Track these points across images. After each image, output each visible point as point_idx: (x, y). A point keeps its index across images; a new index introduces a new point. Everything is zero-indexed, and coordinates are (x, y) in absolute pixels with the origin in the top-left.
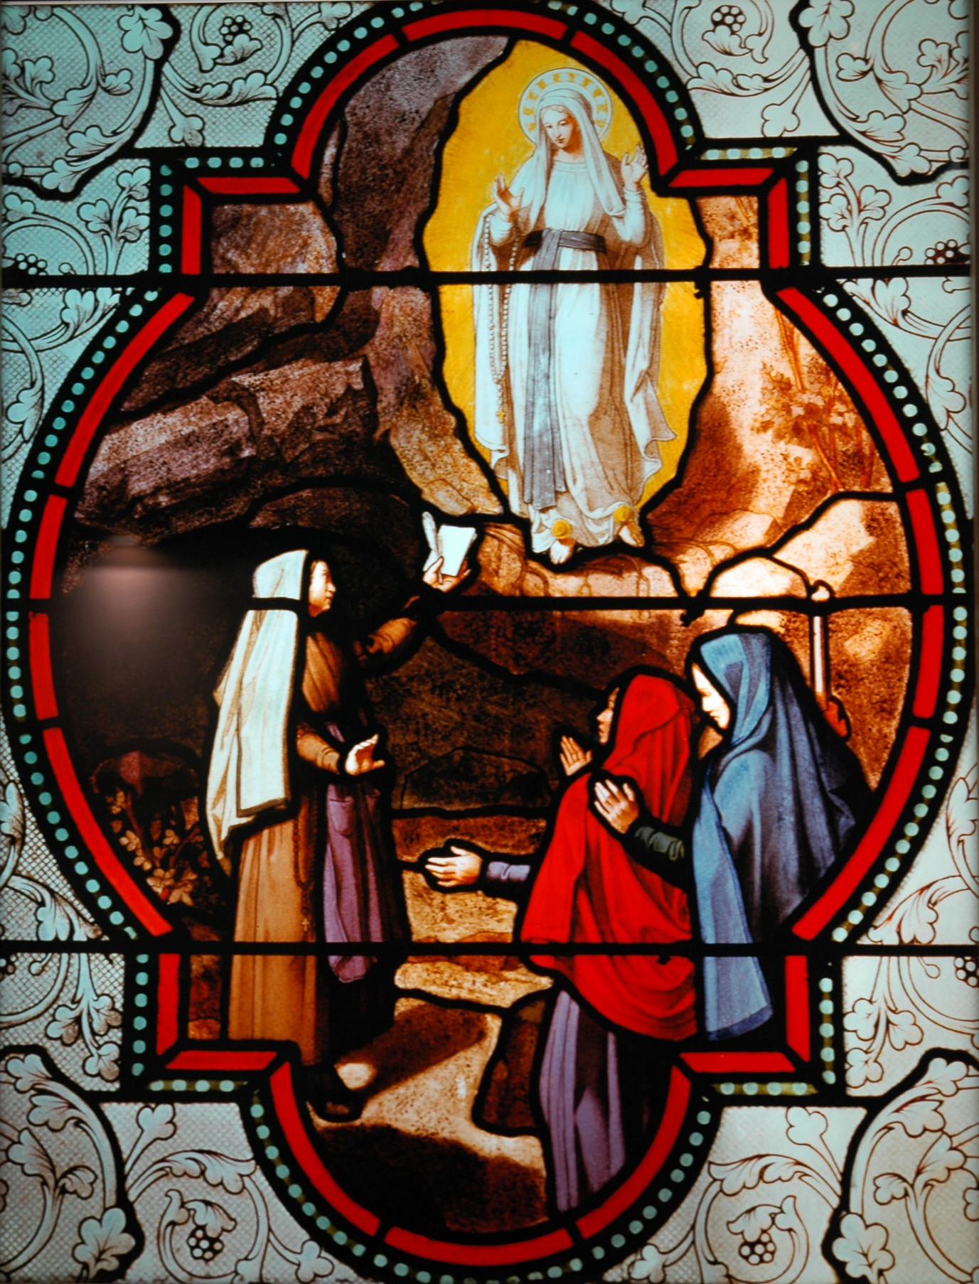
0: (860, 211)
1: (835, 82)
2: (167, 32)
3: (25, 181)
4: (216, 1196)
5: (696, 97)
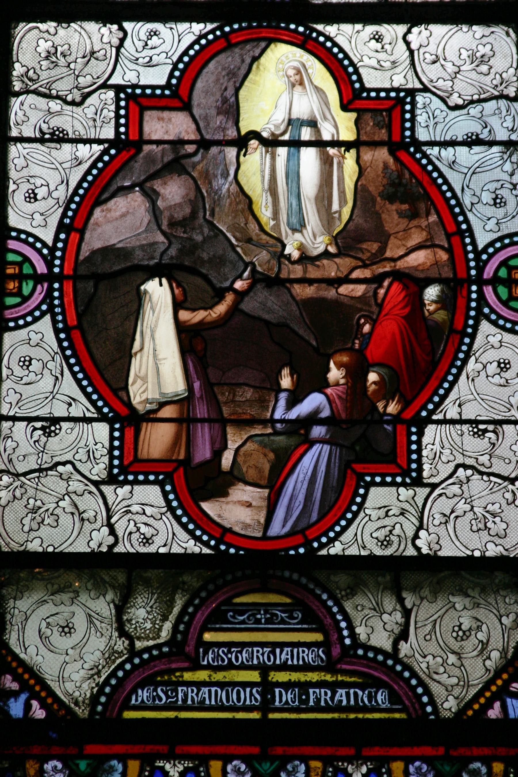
0: (434, 118)
1: (423, 64)
2: (121, 35)
3: (58, 97)
4: (151, 521)
5: (361, 70)
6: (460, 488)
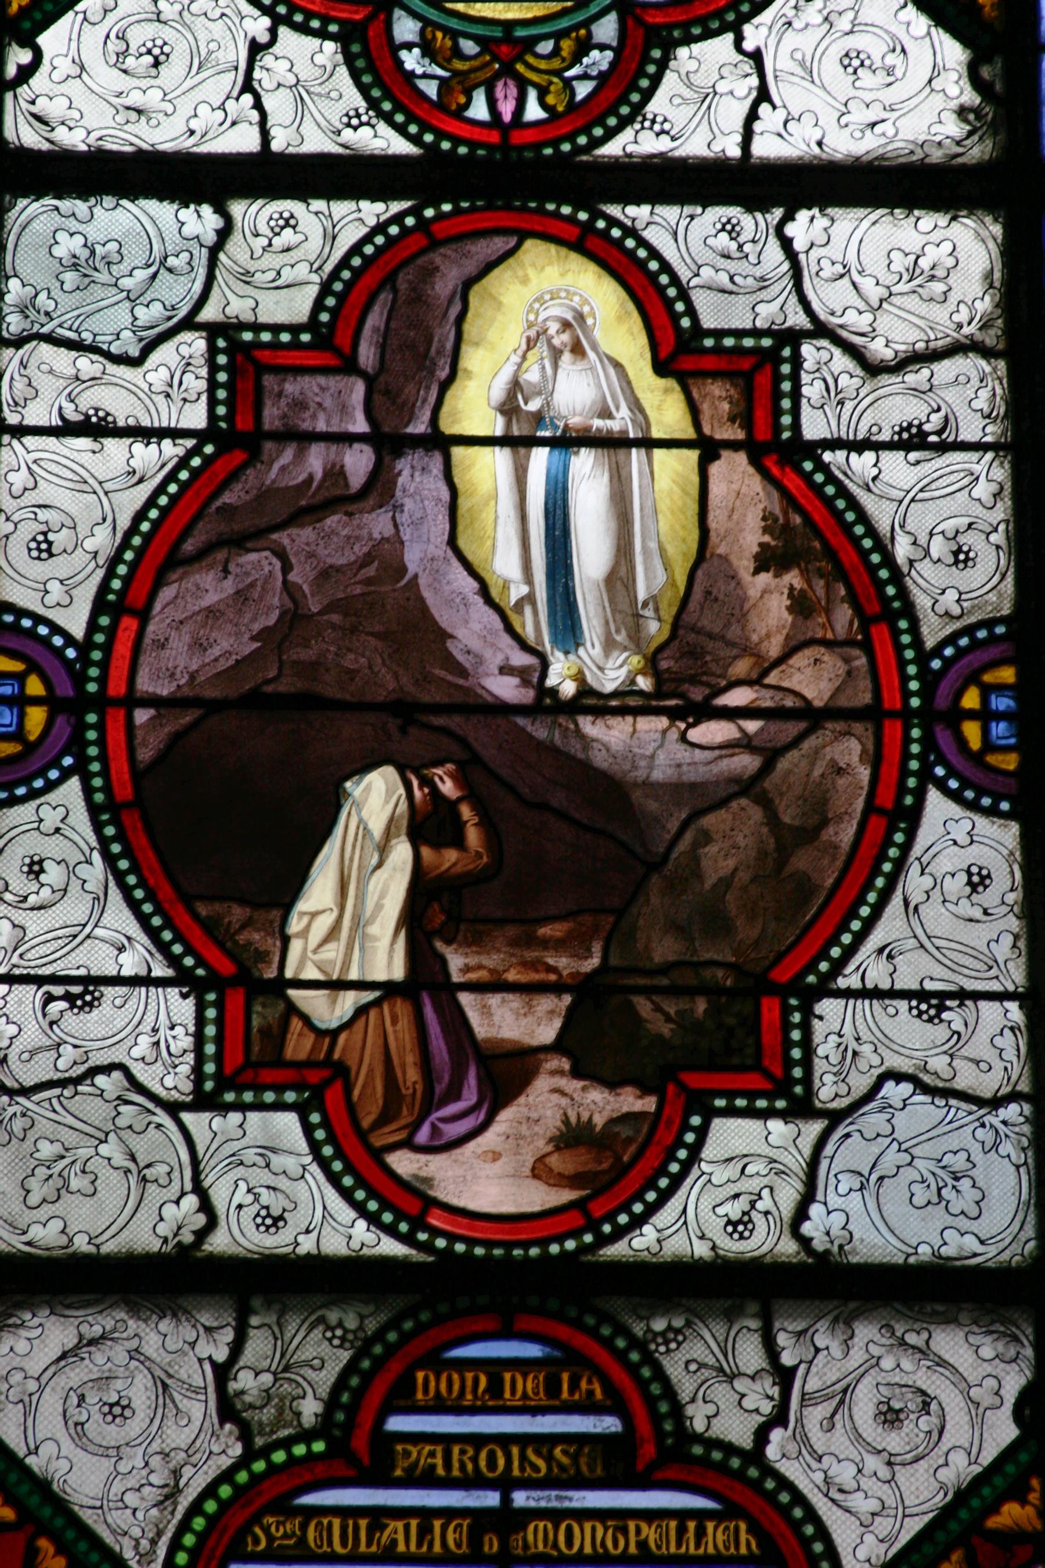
3: (93, 349)
4: (282, 1183)
6: (889, 1121)
